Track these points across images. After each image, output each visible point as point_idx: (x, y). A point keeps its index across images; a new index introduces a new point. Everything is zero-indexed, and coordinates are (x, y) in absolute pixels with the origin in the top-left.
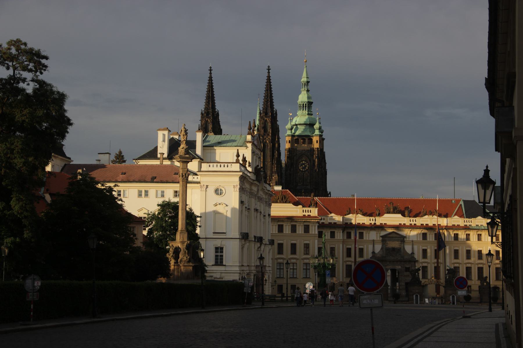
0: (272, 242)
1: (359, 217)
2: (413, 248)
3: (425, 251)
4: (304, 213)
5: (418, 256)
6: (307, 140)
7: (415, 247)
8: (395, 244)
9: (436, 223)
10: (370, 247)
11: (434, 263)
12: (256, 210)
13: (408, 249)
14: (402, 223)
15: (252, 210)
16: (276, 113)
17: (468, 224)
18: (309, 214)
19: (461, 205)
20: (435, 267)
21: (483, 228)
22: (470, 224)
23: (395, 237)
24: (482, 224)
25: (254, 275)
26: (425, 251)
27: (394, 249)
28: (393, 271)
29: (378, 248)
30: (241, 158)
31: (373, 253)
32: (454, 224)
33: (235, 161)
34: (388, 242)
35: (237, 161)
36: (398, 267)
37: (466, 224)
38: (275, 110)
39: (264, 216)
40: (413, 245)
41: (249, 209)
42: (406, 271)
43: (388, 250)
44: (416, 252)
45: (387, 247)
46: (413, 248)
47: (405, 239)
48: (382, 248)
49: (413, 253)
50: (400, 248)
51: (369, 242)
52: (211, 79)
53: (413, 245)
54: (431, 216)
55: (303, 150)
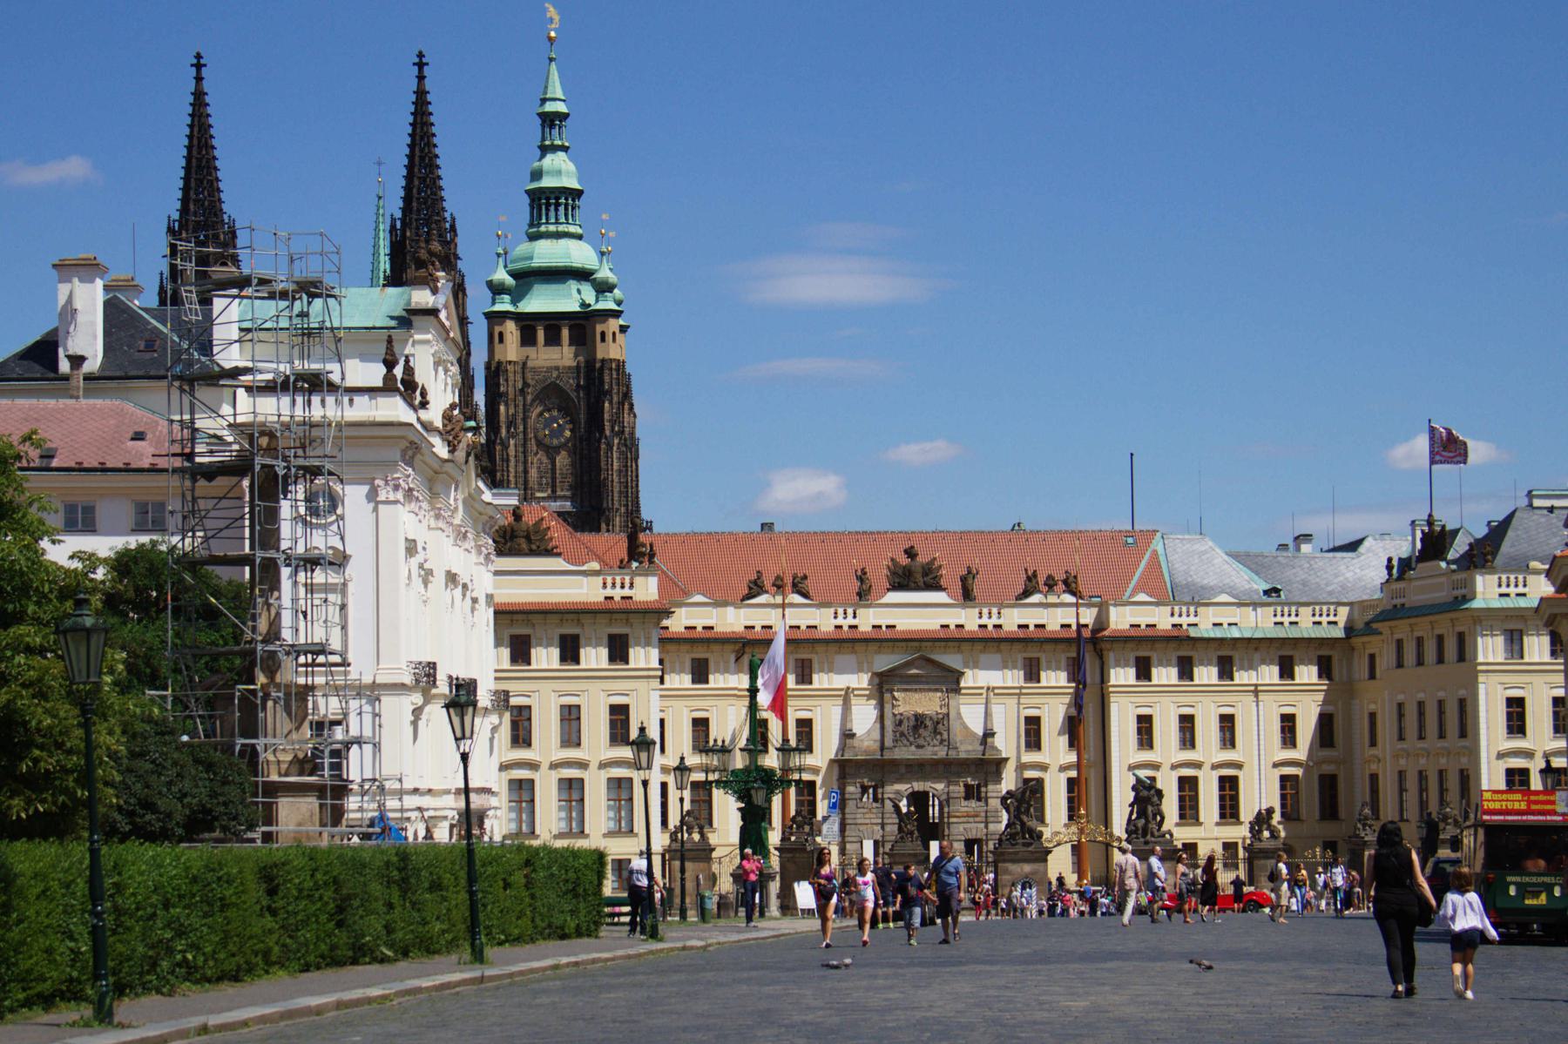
0: (502, 699)
1: (792, 605)
2: (987, 714)
3: (1033, 727)
4: (609, 592)
5: (1007, 742)
6: (565, 333)
7: (998, 711)
8: (926, 703)
9: (1073, 622)
10: (836, 712)
11: (1063, 769)
12: (452, 578)
13: (970, 716)
14: (952, 623)
15: (439, 579)
16: (453, 228)
17: (1184, 621)
18: (627, 592)
19: (1155, 552)
20: (1071, 781)
21: (1235, 633)
22: (1192, 620)
24: (1232, 620)
25: (452, 826)
26: (1033, 725)
27: (919, 721)
28: (919, 799)
29: (864, 718)
30: (398, 371)
31: (847, 735)
32: (1135, 621)
33: (380, 384)
35: (388, 387)
37: (1176, 620)
38: (447, 215)
39: (475, 601)
41: (430, 572)
42: (967, 798)
44: (998, 726)
46: (987, 714)
48: (881, 717)
49: (989, 734)
51: (828, 694)
54: (1052, 599)
55: (550, 369)
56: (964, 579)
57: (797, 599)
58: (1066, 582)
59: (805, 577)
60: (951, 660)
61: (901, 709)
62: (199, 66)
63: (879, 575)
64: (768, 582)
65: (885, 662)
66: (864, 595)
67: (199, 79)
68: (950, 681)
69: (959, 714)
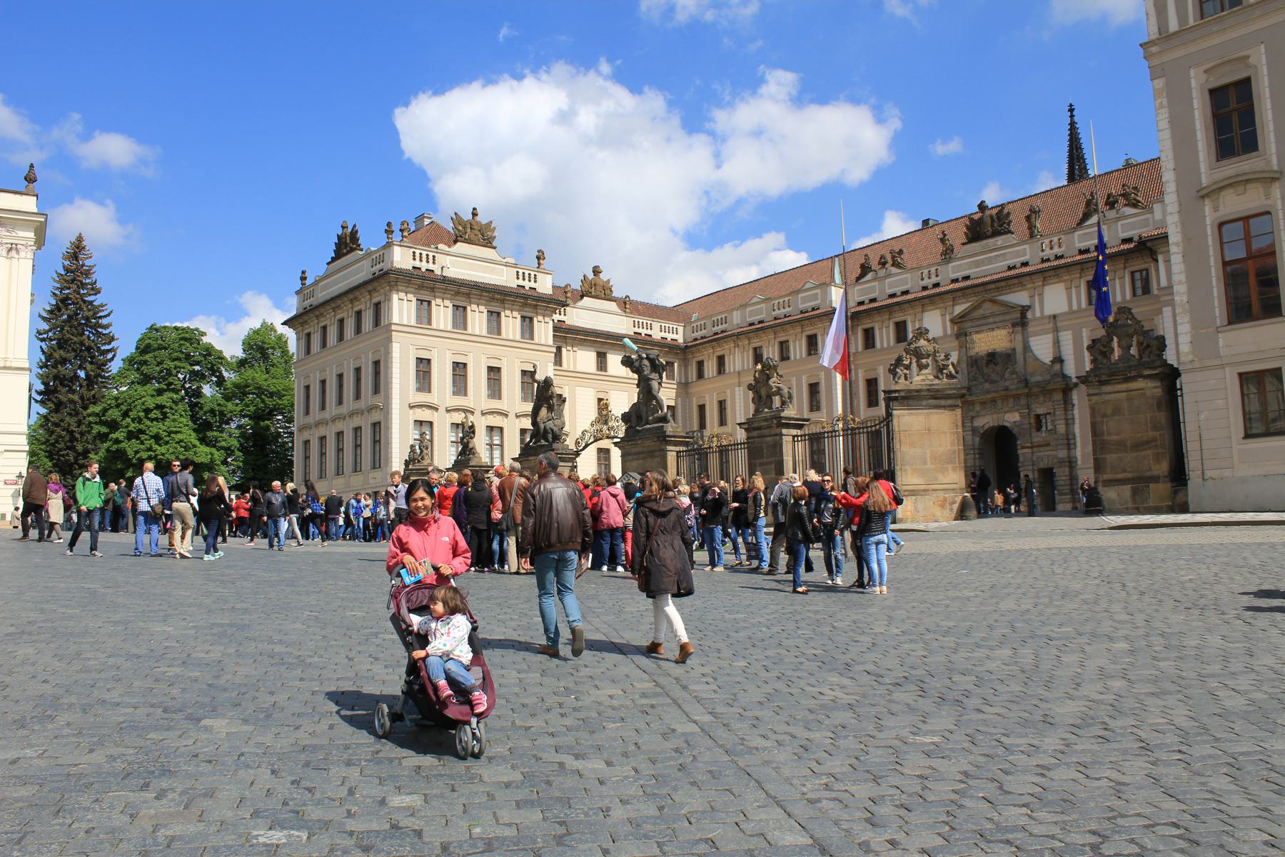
1: (889, 275)
2: (1057, 343)
7: (1066, 338)
13: (1042, 348)
23: (993, 315)
27: (992, 357)
34: (975, 337)
36: (1011, 418)
40: (1056, 330)
43: (974, 362)
45: (972, 353)
46: (1057, 343)
47: (1029, 315)
49: (1059, 360)
50: (1014, 350)
52: (1073, 125)
53: (1056, 330)
56: (1028, 218)
57: (894, 270)
58: (1124, 195)
59: (901, 252)
60: (1019, 298)
61: (977, 350)
62: (1071, 110)
63: (957, 236)
64: (874, 264)
65: (959, 309)
66: (948, 254)
67: (1072, 116)
68: (1021, 318)
69: (1027, 348)
